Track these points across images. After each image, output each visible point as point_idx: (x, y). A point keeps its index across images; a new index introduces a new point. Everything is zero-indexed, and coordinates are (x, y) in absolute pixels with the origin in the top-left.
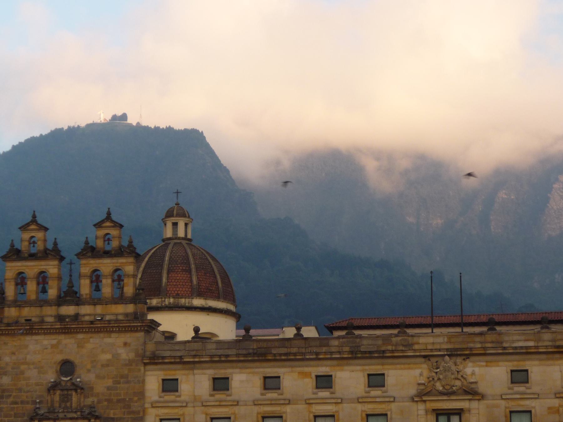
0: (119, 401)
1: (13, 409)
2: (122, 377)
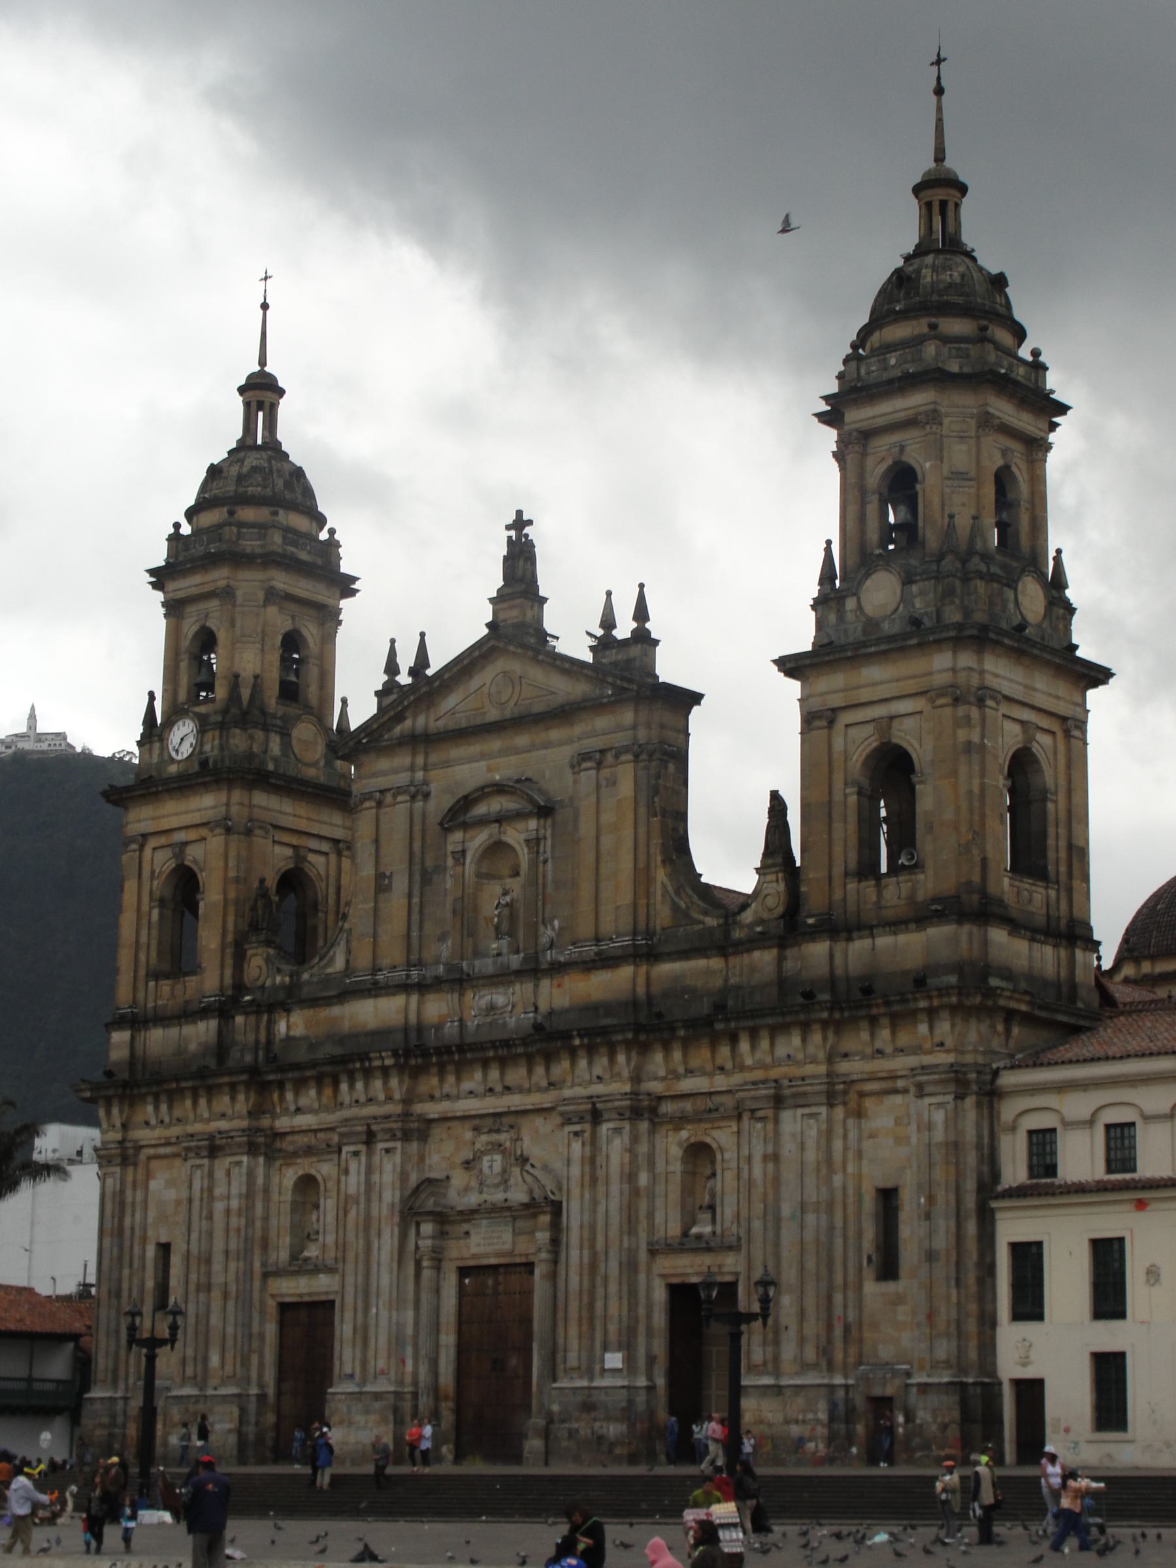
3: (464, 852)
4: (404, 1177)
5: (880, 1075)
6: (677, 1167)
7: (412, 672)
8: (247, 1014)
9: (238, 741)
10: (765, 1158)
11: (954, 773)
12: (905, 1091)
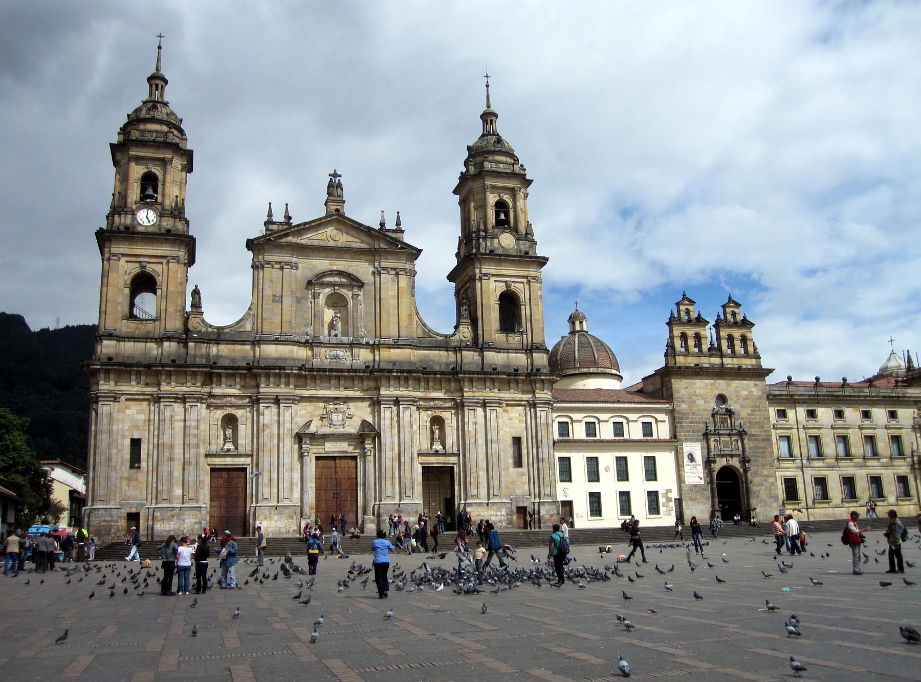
0: (756, 423)
2: (756, 407)
6: (429, 424)
8: (196, 342)
11: (538, 305)
12: (524, 405)
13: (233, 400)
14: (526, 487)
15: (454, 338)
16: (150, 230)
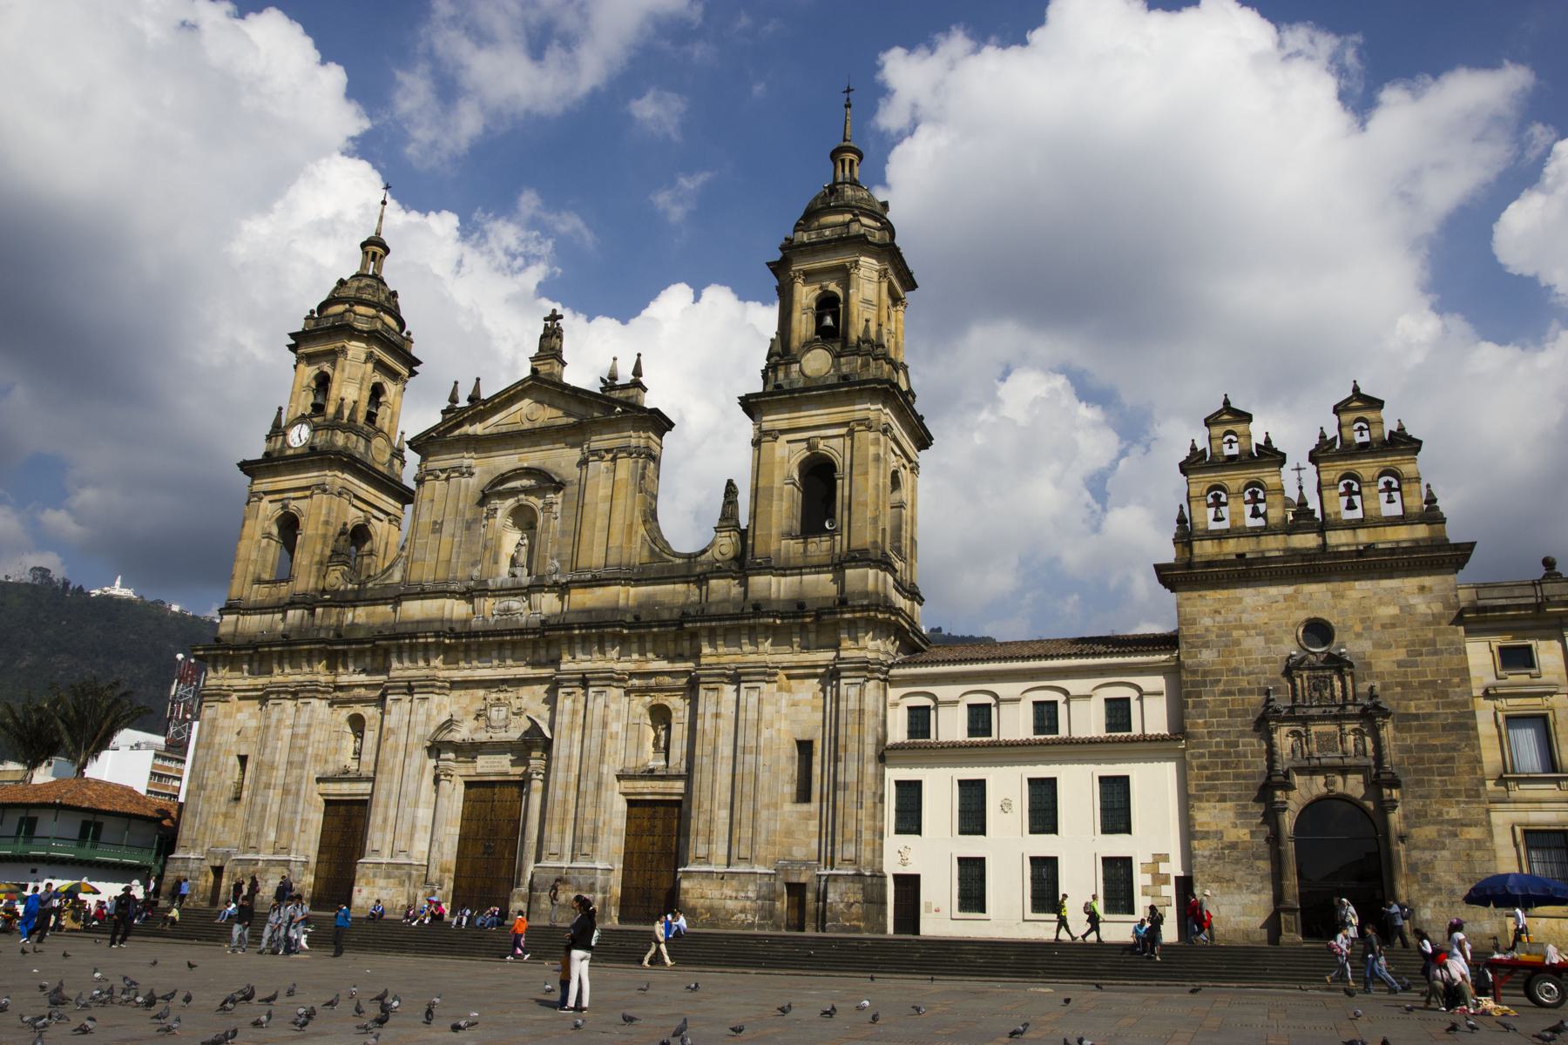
0: (1423, 685)
1: (1225, 703)
2: (1424, 643)
3: (496, 509)
4: (428, 716)
5: (805, 664)
7: (470, 399)
8: (324, 606)
9: (340, 439)
10: (717, 715)
11: (866, 473)
13: (363, 691)
14: (815, 846)
15: (703, 557)
16: (299, 451)
